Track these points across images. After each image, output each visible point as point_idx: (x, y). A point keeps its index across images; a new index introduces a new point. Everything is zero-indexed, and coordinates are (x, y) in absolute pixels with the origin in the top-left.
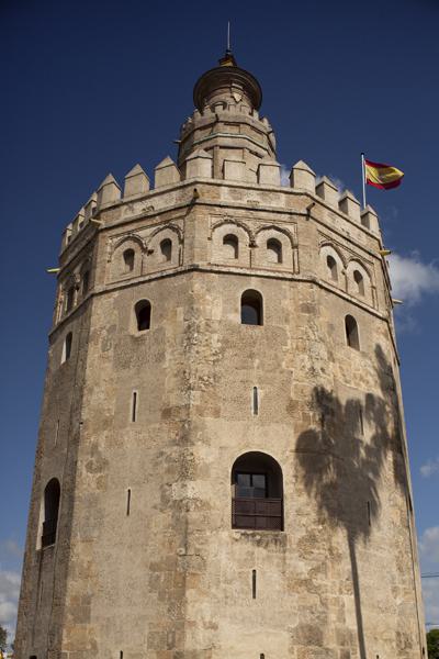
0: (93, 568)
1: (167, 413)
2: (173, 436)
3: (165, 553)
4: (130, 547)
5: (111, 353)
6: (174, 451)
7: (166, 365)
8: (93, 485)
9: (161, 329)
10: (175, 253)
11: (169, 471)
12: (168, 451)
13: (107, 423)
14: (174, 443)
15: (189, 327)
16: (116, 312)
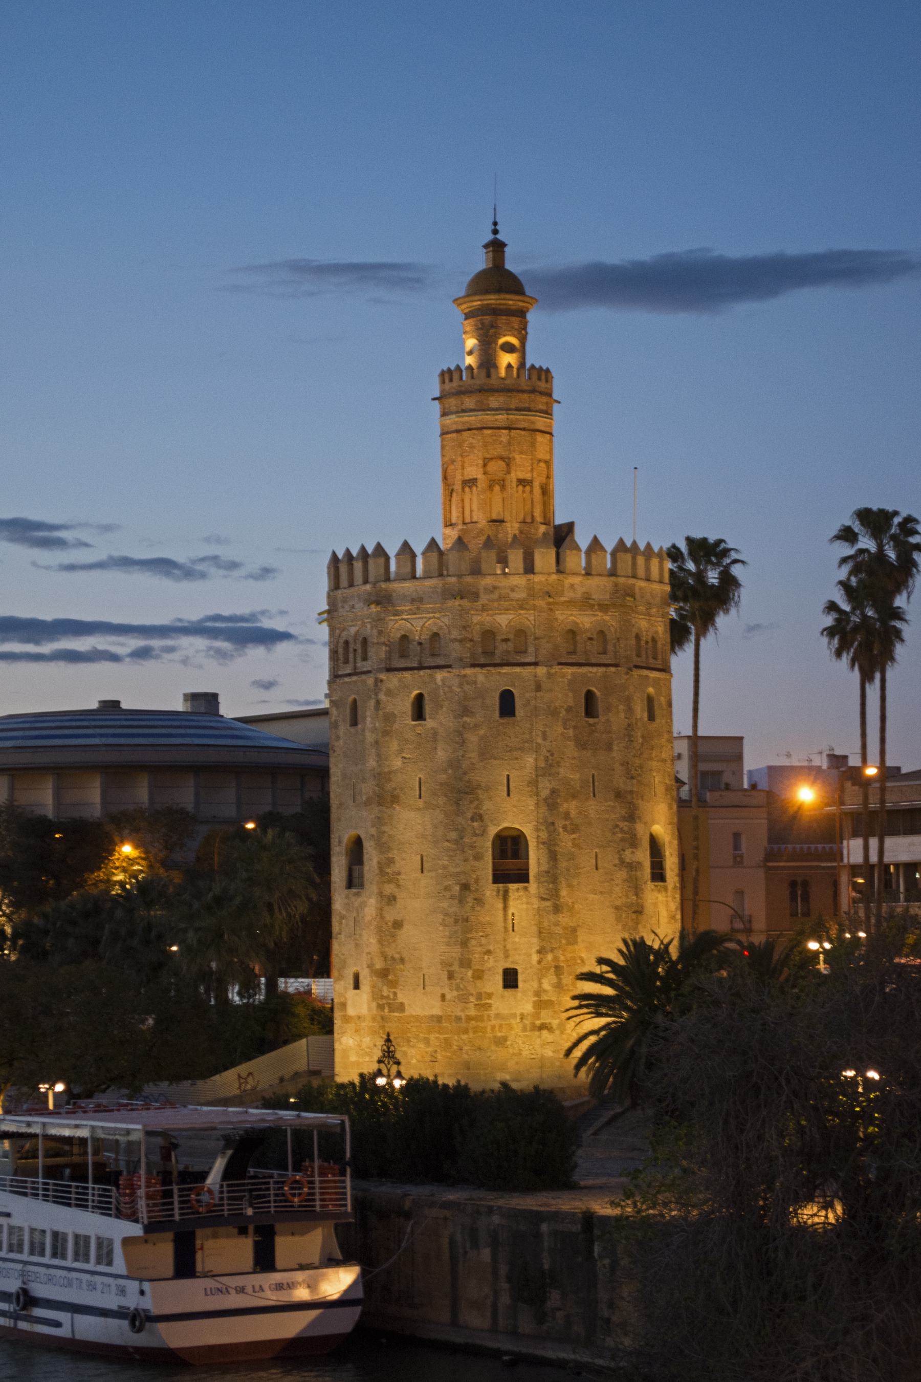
0: (576, 906)
1: (618, 795)
2: (623, 813)
3: (624, 899)
4: (601, 892)
5: (571, 732)
6: (624, 825)
7: (614, 754)
8: (570, 844)
9: (608, 721)
10: (610, 648)
11: (622, 840)
12: (621, 824)
13: (574, 796)
14: (624, 819)
15: (629, 725)
16: (570, 694)
